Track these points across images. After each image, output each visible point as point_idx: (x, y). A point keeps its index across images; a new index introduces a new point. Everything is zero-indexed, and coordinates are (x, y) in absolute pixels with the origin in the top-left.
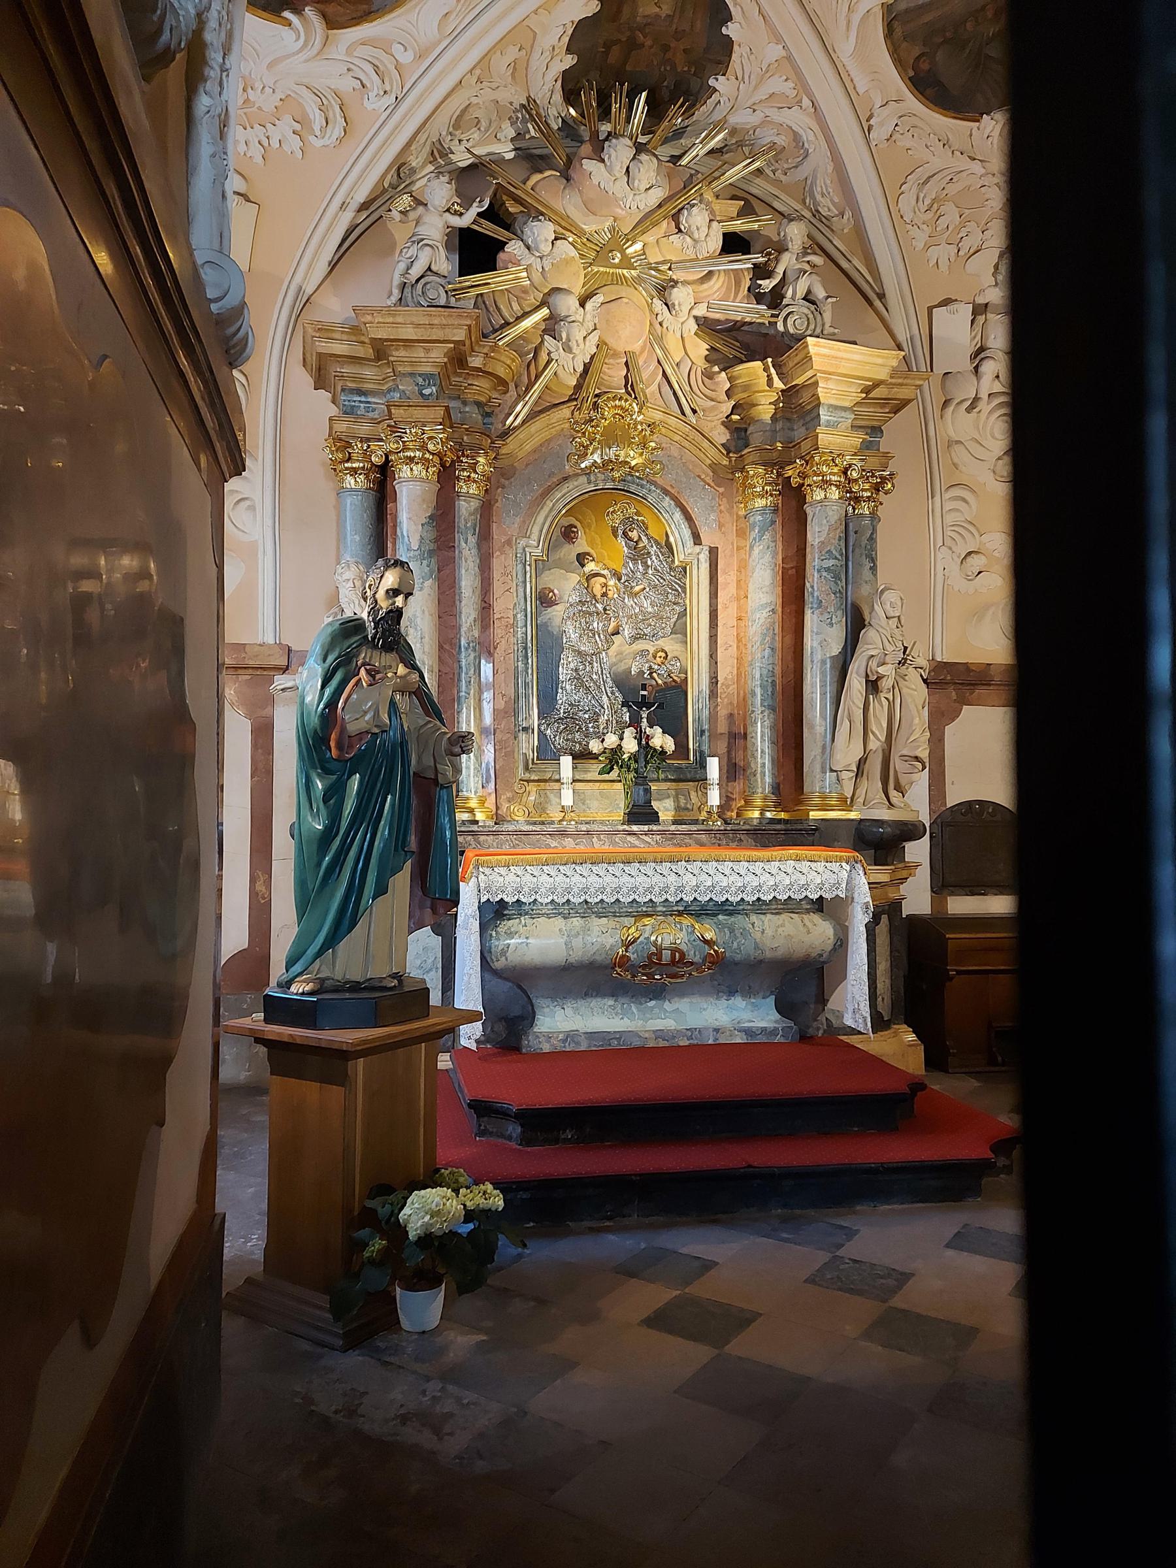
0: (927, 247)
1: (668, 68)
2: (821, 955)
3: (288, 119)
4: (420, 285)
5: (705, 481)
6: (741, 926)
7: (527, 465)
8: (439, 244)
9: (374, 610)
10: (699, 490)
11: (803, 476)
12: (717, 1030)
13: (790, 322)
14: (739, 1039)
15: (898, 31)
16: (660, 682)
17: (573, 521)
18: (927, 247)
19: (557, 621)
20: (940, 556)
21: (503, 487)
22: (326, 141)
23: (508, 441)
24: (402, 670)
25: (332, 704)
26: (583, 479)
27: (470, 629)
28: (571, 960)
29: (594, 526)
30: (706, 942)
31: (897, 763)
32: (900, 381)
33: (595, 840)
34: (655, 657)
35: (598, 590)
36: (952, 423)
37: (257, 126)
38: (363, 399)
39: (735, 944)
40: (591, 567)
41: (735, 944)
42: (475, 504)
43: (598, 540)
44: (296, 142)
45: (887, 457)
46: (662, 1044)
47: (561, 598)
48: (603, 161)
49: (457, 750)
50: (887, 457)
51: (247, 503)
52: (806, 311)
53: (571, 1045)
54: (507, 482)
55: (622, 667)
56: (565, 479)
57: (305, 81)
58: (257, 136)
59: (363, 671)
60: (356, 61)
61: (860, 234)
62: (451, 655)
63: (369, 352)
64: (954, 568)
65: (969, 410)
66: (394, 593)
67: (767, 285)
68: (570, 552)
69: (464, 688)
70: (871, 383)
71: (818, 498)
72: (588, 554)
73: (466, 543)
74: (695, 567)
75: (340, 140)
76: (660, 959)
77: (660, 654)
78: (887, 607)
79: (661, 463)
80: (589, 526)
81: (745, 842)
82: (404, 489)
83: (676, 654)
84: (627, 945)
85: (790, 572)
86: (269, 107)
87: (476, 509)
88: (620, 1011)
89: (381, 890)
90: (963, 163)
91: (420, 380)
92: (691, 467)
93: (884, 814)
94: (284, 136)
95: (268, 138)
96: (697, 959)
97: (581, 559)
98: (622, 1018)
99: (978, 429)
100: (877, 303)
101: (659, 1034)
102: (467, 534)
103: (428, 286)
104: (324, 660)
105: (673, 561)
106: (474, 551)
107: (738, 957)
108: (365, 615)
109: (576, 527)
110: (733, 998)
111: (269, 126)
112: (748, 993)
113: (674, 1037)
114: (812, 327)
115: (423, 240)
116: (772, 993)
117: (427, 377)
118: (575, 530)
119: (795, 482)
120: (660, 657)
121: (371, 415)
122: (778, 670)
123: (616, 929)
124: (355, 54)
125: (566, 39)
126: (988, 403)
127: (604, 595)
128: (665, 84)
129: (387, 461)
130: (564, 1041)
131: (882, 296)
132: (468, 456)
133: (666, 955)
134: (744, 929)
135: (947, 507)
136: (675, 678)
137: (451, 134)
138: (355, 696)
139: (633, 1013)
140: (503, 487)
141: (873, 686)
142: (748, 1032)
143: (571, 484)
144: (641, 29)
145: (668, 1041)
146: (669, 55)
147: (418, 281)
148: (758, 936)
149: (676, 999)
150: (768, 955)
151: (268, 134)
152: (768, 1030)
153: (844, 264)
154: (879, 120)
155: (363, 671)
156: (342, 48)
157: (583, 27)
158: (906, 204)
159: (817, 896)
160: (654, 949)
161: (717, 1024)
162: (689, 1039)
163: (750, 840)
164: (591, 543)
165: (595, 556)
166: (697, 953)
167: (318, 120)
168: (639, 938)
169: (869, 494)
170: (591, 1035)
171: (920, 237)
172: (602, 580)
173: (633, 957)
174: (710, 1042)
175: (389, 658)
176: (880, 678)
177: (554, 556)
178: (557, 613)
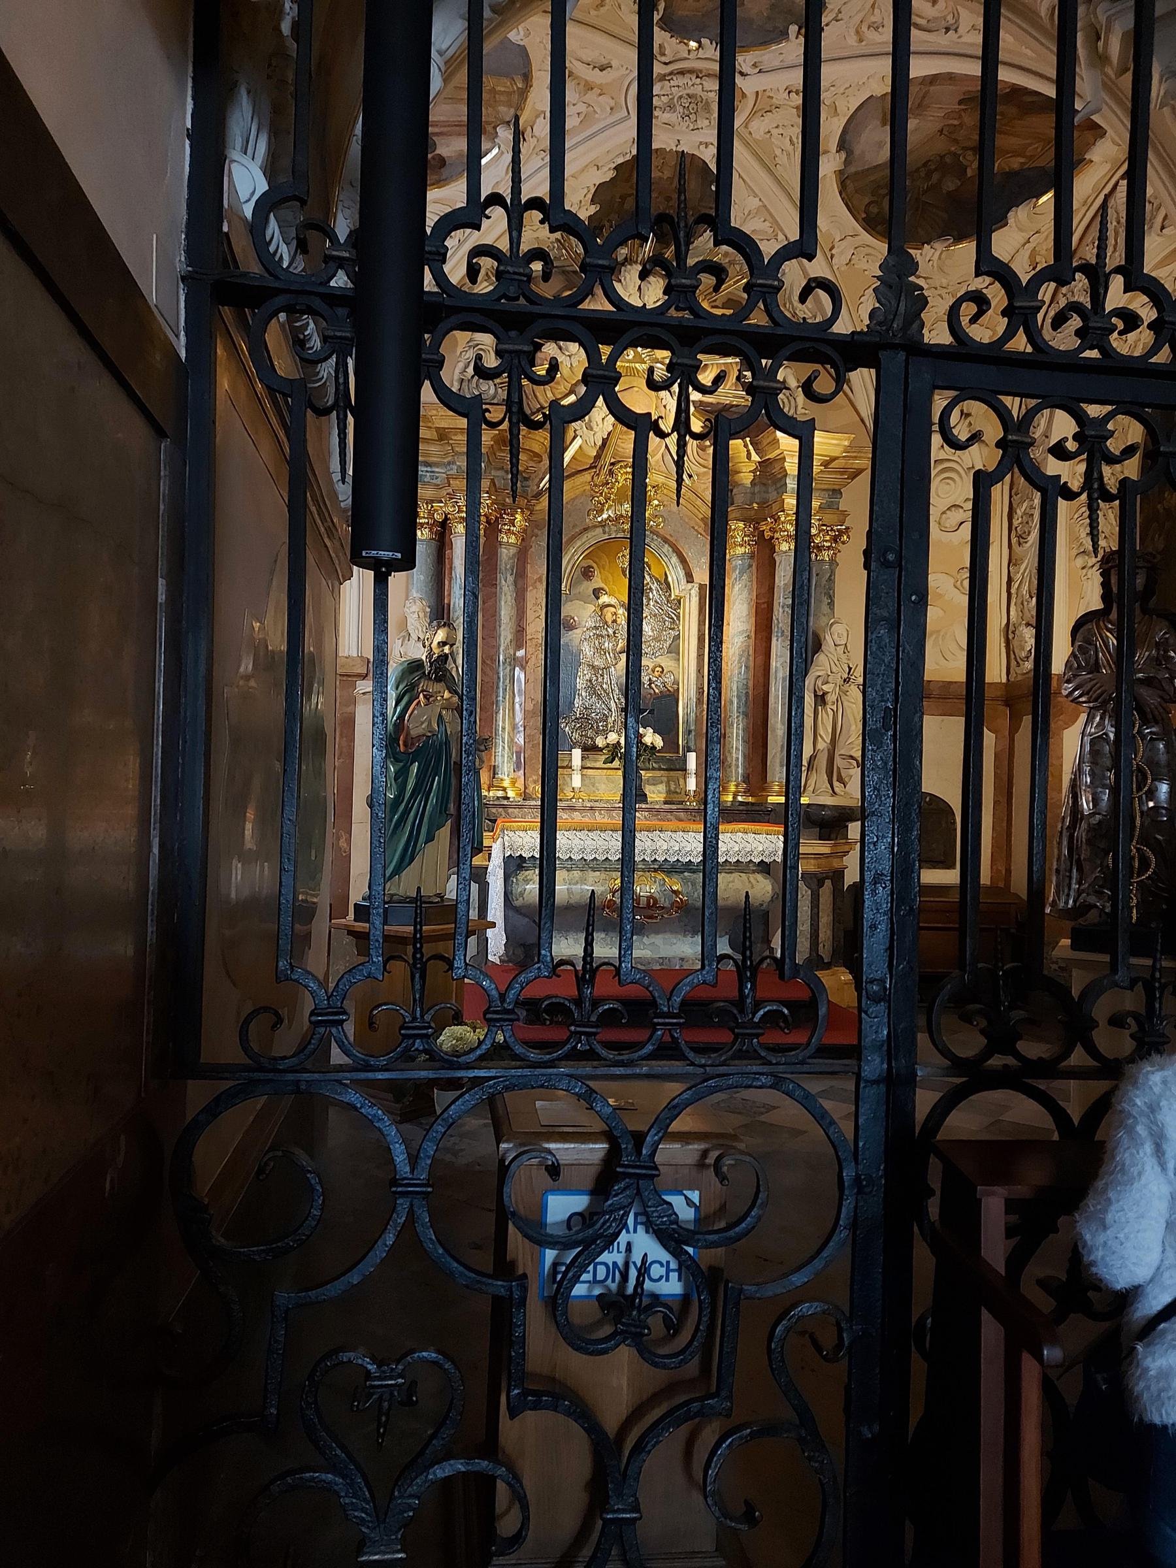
5: (696, 531)
8: (490, 349)
9: (430, 655)
11: (773, 530)
12: (682, 959)
15: (851, 186)
16: (657, 691)
17: (590, 563)
24: (447, 695)
25: (401, 717)
26: (600, 530)
27: (507, 648)
28: (572, 901)
29: (607, 568)
30: (674, 892)
31: (838, 761)
32: (855, 454)
33: (597, 814)
34: (653, 671)
38: (429, 469)
40: (604, 599)
42: (513, 551)
45: (845, 514)
49: (482, 748)
50: (845, 514)
54: (539, 533)
56: (586, 530)
59: (421, 695)
62: (492, 669)
63: (435, 436)
66: (442, 644)
68: (588, 587)
69: (501, 694)
71: (784, 549)
72: (603, 589)
74: (687, 600)
77: (658, 669)
78: (835, 637)
79: (662, 516)
82: (459, 542)
85: (763, 606)
89: (430, 838)
93: (829, 801)
96: (667, 904)
97: (597, 593)
104: (397, 689)
105: (670, 595)
106: (512, 588)
108: (424, 658)
115: (478, 345)
119: (767, 535)
121: (434, 481)
122: (751, 684)
125: (590, 196)
127: (614, 621)
129: (446, 519)
132: (508, 515)
138: (416, 712)
141: (820, 699)
143: (590, 534)
154: (840, 250)
155: (421, 695)
159: (759, 860)
161: (683, 955)
162: (661, 964)
164: (605, 581)
169: (829, 544)
172: (613, 609)
174: (677, 967)
175: (439, 686)
176: (825, 694)
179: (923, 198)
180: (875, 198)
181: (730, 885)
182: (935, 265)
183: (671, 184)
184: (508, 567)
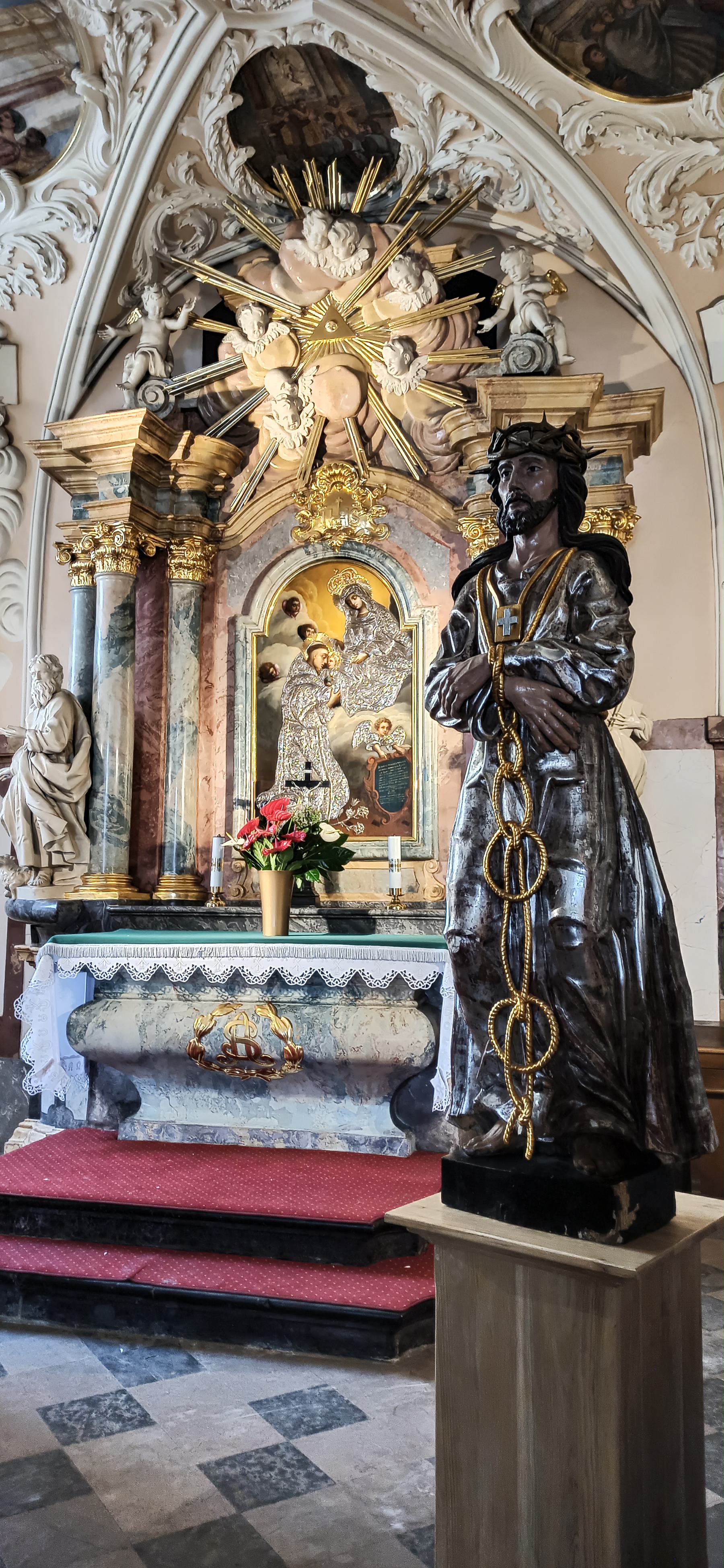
0: (677, 246)
1: (346, 134)
2: (411, 1060)
4: (140, 391)
5: (434, 539)
6: (322, 1021)
7: (252, 544)
8: (155, 351)
10: (428, 549)
12: (315, 1135)
13: (511, 360)
14: (341, 1147)
16: (382, 754)
17: (294, 593)
18: (677, 246)
19: (277, 696)
21: (229, 568)
22: (53, 280)
23: (230, 523)
28: (147, 1047)
33: (247, 922)
34: (377, 727)
35: (319, 662)
39: (313, 1043)
40: (311, 640)
41: (313, 1043)
43: (320, 610)
44: (31, 283)
46: (257, 1144)
47: (282, 672)
48: (303, 238)
52: (531, 344)
53: (165, 1137)
55: (342, 741)
56: (288, 553)
57: (24, 232)
61: (598, 249)
67: (488, 324)
68: (291, 625)
70: (574, 413)
72: (309, 626)
73: (178, 626)
76: (235, 1051)
77: (386, 725)
79: (387, 525)
80: (311, 597)
81: (408, 928)
83: (400, 723)
84: (201, 1035)
87: (191, 594)
88: (224, 1105)
90: (691, 148)
91: (114, 480)
92: (419, 526)
94: (21, 282)
95: (10, 286)
96: (274, 1055)
97: (302, 631)
98: (226, 1113)
100: (640, 317)
101: (254, 1134)
102: (178, 617)
103: (147, 391)
106: (187, 634)
107: (318, 1056)
109: (297, 600)
110: (343, 1101)
111: (9, 277)
112: (359, 1096)
113: (270, 1138)
114: (538, 359)
116: (385, 1099)
117: (119, 477)
118: (297, 603)
120: (383, 727)
123: (191, 1017)
124: (53, 198)
125: (226, 136)
127: (326, 666)
128: (354, 148)
130: (159, 1131)
131: (642, 310)
133: (241, 1049)
134: (325, 1025)
136: (399, 749)
137: (166, 244)
139: (237, 1108)
140: (229, 568)
142: (351, 1141)
144: (297, 104)
145: (263, 1141)
146: (338, 122)
147: (138, 387)
148: (338, 1033)
149: (281, 1097)
150: (351, 1055)
151: (10, 283)
152: (373, 1140)
153: (601, 283)
154: (568, 128)
157: (234, 119)
158: (636, 205)
160: (227, 1042)
162: (286, 1141)
163: (413, 927)
164: (314, 616)
165: (316, 626)
166: (273, 1048)
168: (211, 1029)
170: (186, 1128)
171: (666, 238)
172: (323, 651)
173: (207, 1048)
174: (309, 1147)
177: (277, 631)
178: (277, 688)
179: (665, 21)
180: (591, 42)
181: (363, 1028)
182: (717, 115)
183: (319, 95)
184: (181, 609)
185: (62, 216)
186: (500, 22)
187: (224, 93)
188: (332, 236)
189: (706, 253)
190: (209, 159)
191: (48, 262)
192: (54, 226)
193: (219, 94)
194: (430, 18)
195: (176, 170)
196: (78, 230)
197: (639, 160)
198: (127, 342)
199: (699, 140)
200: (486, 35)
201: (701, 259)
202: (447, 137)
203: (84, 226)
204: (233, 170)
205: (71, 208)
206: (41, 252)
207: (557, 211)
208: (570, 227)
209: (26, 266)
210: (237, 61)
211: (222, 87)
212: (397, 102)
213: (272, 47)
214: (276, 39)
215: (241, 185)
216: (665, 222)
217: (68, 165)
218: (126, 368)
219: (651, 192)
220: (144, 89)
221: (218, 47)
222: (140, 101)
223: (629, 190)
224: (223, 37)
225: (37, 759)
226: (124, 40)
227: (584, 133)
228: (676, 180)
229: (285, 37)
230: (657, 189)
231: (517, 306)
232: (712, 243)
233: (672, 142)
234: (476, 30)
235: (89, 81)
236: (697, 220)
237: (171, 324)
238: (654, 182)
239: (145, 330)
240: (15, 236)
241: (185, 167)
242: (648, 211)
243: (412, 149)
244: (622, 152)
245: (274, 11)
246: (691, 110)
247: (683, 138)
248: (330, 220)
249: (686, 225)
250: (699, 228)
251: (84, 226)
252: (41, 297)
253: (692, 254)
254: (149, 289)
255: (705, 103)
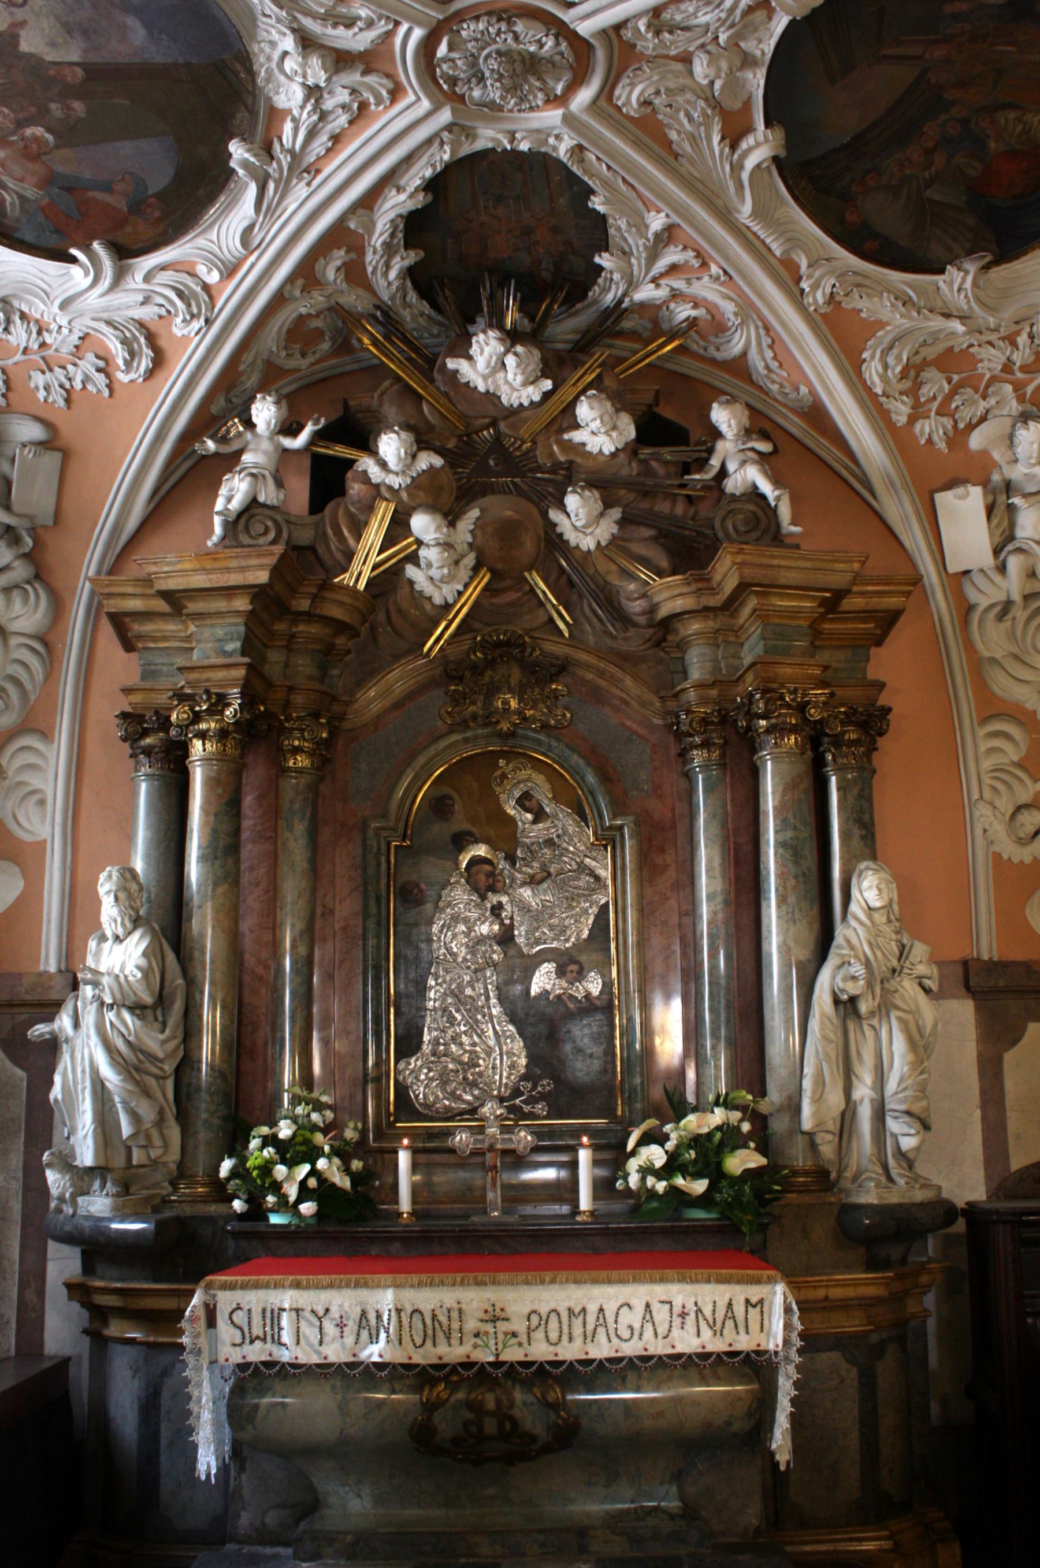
3: (90, 356)
18: (912, 419)
20: (977, 814)
22: (133, 376)
36: (981, 635)
37: (57, 369)
44: (101, 379)
51: (37, 797)
57: (105, 316)
58: (57, 379)
60: (158, 289)
64: (999, 829)
65: (1001, 617)
75: (150, 374)
86: (66, 349)
90: (937, 323)
95: (70, 379)
99: (1016, 640)
111: (70, 367)
124: (156, 281)
126: (1025, 608)
135: (982, 748)
154: (811, 282)
156: (139, 276)
158: (872, 371)
167: (118, 353)
185: (162, 301)
186: (765, 165)
187: (417, 190)
188: (510, 361)
189: (941, 432)
190: (369, 257)
191: (132, 354)
192: (146, 313)
193: (411, 189)
194: (688, 149)
195: (327, 264)
196: (184, 321)
197: (881, 324)
198: (229, 461)
199: (947, 316)
200: (745, 176)
201: (935, 438)
202: (663, 270)
203: (193, 316)
204: (393, 274)
205: (180, 294)
206: (125, 342)
207: (774, 365)
208: (785, 384)
209: (98, 357)
210: (446, 157)
211: (418, 182)
212: (619, 225)
213: (493, 150)
214: (499, 142)
215: (398, 290)
216: (901, 393)
217: (188, 245)
218: (223, 491)
219: (891, 360)
220: (318, 171)
221: (428, 142)
222: (309, 184)
223: (865, 355)
224: (442, 130)
225: (119, 1015)
226: (315, 118)
227: (828, 290)
228: (917, 353)
229: (511, 142)
230: (899, 358)
231: (731, 467)
232: (948, 423)
233: (919, 313)
234: (737, 168)
235: (255, 155)
236: (934, 398)
237: (289, 443)
238: (895, 351)
239: (251, 447)
240: (93, 319)
241: (339, 263)
242: (884, 378)
243: (616, 276)
244: (863, 315)
245: (516, 114)
246: (941, 284)
247: (931, 311)
248: (508, 342)
249: (922, 400)
250: (935, 405)
251: (193, 316)
252: (111, 395)
253: (927, 430)
254: (264, 398)
255: (959, 280)
